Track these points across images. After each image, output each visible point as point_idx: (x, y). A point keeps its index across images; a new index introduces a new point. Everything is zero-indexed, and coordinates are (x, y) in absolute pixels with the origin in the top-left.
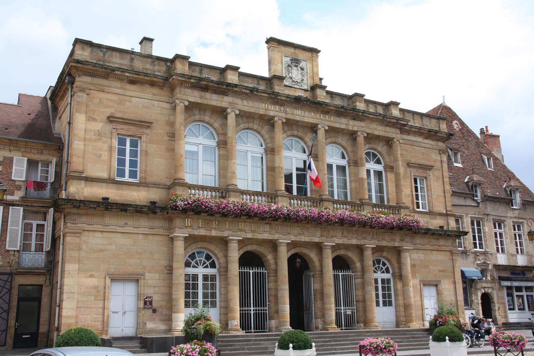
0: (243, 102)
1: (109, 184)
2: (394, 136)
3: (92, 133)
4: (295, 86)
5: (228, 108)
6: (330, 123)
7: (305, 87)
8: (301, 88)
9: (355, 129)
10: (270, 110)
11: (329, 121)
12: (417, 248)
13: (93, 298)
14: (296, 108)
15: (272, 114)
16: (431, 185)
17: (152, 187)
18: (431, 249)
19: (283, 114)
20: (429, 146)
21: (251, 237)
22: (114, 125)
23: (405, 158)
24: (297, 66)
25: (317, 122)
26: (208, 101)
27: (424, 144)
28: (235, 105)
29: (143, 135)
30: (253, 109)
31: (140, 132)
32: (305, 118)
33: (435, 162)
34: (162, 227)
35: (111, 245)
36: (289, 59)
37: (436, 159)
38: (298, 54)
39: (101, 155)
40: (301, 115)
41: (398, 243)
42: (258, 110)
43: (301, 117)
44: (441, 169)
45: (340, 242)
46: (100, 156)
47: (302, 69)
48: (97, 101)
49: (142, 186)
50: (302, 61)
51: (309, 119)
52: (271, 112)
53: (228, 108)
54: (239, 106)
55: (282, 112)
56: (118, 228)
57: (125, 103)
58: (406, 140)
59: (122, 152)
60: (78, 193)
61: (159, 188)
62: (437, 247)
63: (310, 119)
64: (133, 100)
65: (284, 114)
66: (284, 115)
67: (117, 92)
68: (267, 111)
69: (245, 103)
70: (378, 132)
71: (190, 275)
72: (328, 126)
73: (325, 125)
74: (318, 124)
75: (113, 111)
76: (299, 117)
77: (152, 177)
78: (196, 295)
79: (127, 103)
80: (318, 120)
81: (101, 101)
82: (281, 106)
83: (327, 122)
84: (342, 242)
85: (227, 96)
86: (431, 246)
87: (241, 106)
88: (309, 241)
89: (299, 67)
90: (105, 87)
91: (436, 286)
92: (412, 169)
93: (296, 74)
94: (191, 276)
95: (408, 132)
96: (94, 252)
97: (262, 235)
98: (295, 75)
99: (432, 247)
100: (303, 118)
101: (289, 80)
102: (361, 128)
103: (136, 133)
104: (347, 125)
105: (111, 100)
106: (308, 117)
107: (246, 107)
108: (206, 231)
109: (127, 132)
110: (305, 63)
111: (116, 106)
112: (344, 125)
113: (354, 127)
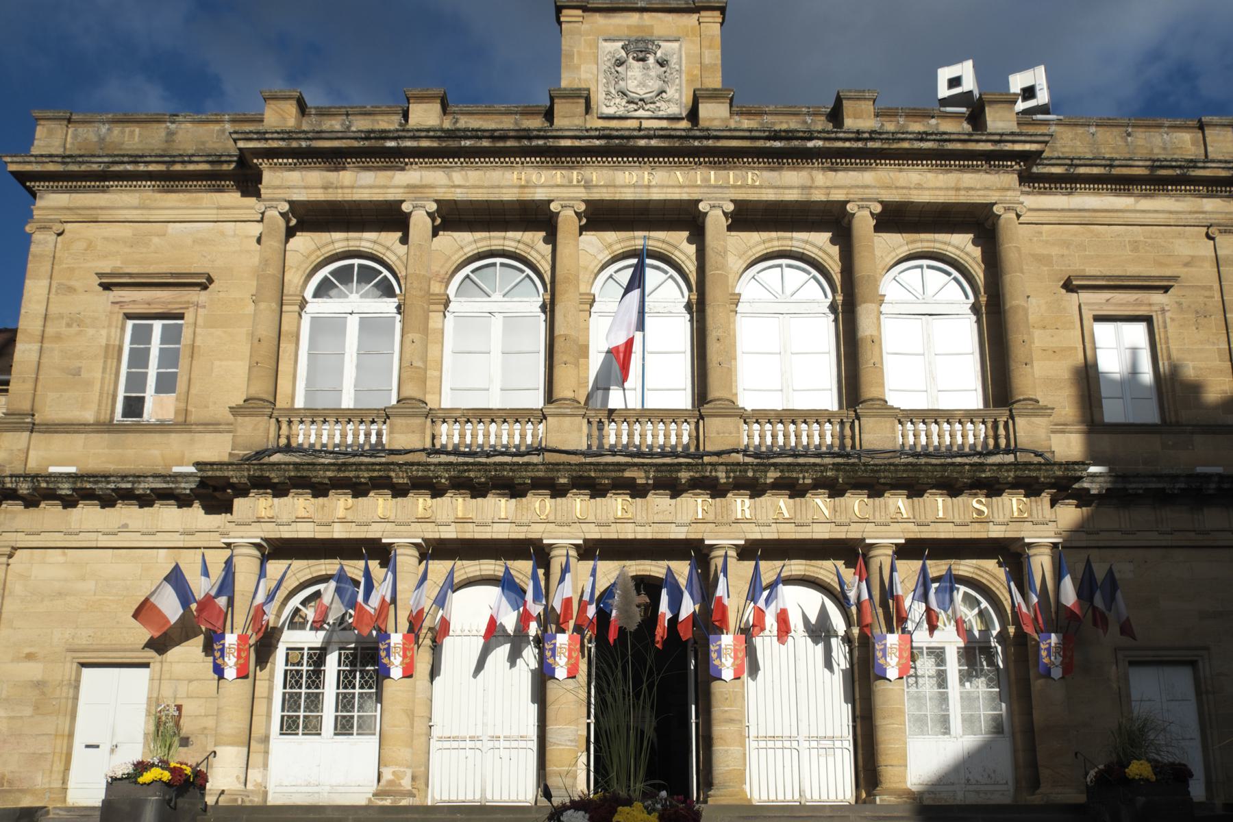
0: (450, 178)
1: (92, 435)
2: (992, 197)
3: (64, 322)
4: (638, 114)
5: (402, 202)
6: (743, 190)
7: (673, 110)
8: (654, 115)
9: (838, 196)
10: (536, 186)
11: (740, 187)
12: (1101, 544)
13: (28, 711)
14: (616, 167)
15: (540, 195)
16: (1167, 339)
17: (200, 432)
18: (1164, 543)
19: (577, 190)
20: (1161, 218)
21: (453, 536)
22: (117, 294)
23: (1056, 267)
24: (643, 60)
25: (695, 197)
26: (346, 191)
27: (1138, 215)
28: (427, 190)
29: (187, 308)
30: (480, 191)
31: (180, 303)
32: (654, 190)
33: (1186, 265)
34: (219, 527)
35: (83, 579)
36: (620, 44)
37: (1193, 257)
38: (652, 26)
39: (80, 368)
40: (640, 183)
41: (1003, 528)
42: (496, 190)
43: (638, 190)
44: (1216, 286)
45: (766, 536)
46: (77, 372)
47: (662, 63)
48: (80, 246)
49: (176, 432)
50: (661, 44)
51: (665, 190)
52: (539, 190)
53: (402, 202)
54: (438, 190)
55: (575, 186)
56: (101, 537)
57: (150, 240)
58: (1062, 210)
59: (139, 358)
60: (11, 463)
61: (220, 432)
62: (1192, 535)
63: (670, 190)
64: (170, 231)
65: (583, 190)
66: (583, 194)
67: (130, 218)
68: (526, 190)
69: (458, 177)
70: (927, 192)
71: (302, 649)
72: (732, 201)
73: (723, 199)
74: (698, 201)
75: (119, 264)
76: (632, 190)
77: (207, 407)
78: (315, 702)
79: (156, 240)
80: (697, 190)
81: (90, 246)
82: (571, 168)
83: (732, 190)
84: (775, 536)
85: (403, 169)
86: (1161, 533)
87: (443, 190)
88: (649, 536)
89: (651, 60)
90: (99, 211)
91: (1193, 664)
92: (1085, 296)
93: (638, 79)
94: (306, 652)
95: (1069, 181)
96: (42, 601)
97: (489, 529)
98: (636, 83)
99: (1169, 537)
100: (645, 190)
101: (618, 101)
102: (860, 191)
103: (170, 306)
104: (803, 188)
105: (115, 240)
106: (662, 186)
107: (458, 190)
108: (318, 528)
109: (147, 306)
110: (676, 45)
111: (127, 250)
112: (795, 191)
113: (833, 191)
